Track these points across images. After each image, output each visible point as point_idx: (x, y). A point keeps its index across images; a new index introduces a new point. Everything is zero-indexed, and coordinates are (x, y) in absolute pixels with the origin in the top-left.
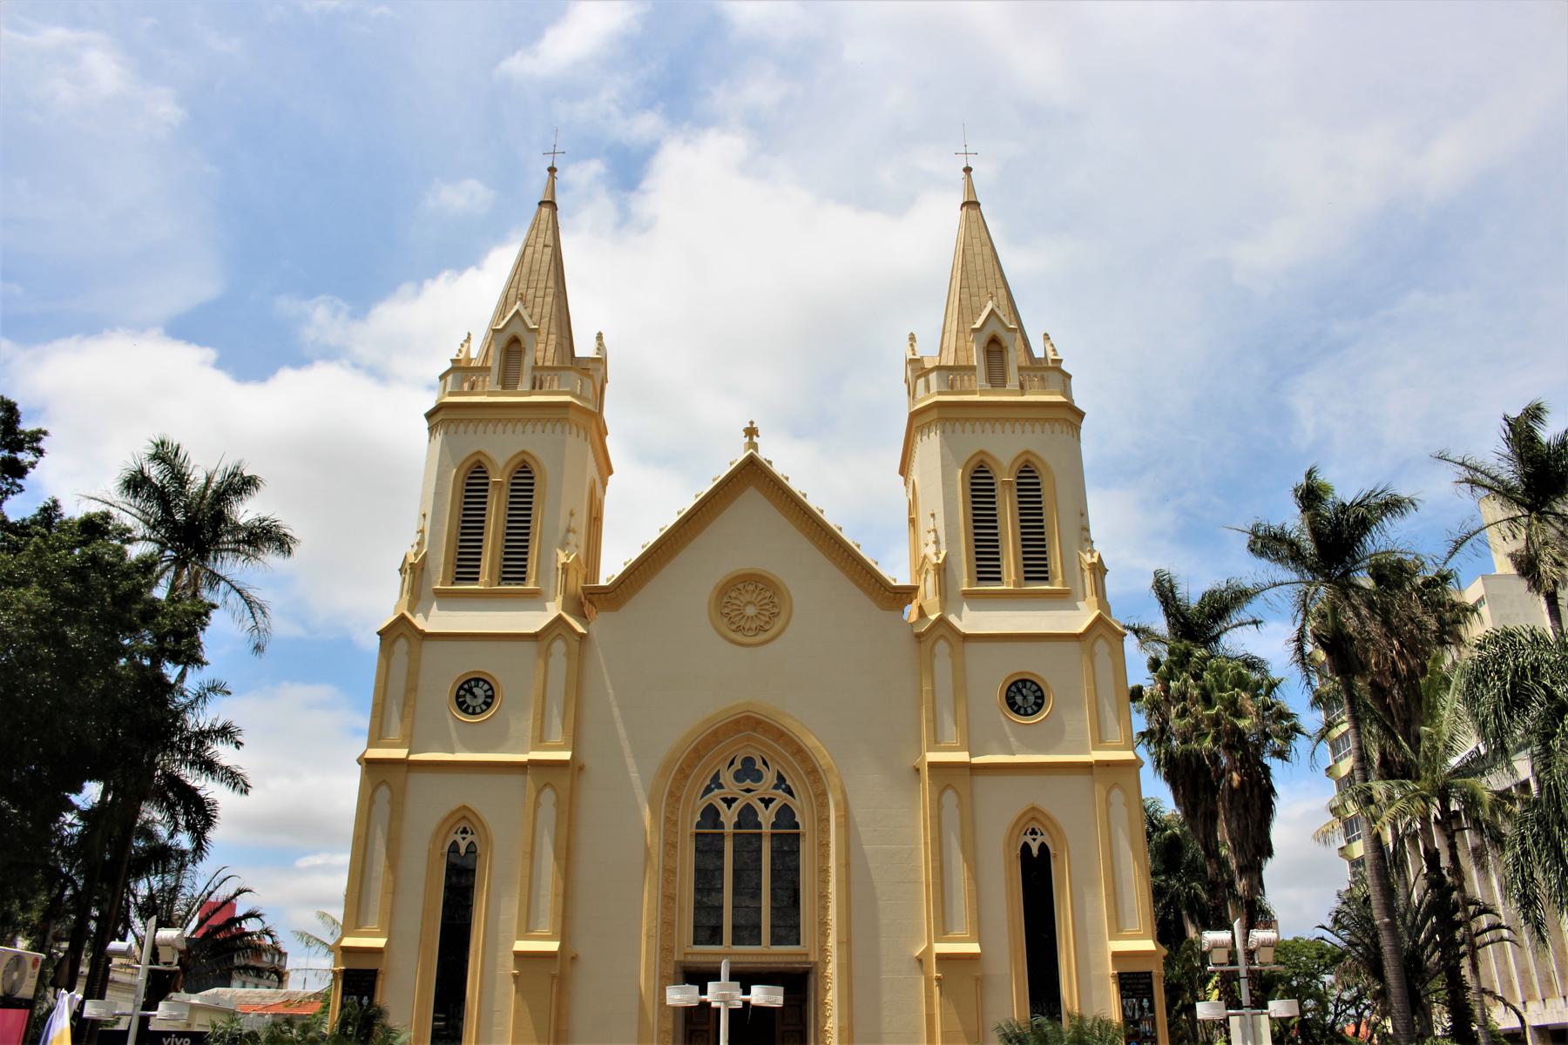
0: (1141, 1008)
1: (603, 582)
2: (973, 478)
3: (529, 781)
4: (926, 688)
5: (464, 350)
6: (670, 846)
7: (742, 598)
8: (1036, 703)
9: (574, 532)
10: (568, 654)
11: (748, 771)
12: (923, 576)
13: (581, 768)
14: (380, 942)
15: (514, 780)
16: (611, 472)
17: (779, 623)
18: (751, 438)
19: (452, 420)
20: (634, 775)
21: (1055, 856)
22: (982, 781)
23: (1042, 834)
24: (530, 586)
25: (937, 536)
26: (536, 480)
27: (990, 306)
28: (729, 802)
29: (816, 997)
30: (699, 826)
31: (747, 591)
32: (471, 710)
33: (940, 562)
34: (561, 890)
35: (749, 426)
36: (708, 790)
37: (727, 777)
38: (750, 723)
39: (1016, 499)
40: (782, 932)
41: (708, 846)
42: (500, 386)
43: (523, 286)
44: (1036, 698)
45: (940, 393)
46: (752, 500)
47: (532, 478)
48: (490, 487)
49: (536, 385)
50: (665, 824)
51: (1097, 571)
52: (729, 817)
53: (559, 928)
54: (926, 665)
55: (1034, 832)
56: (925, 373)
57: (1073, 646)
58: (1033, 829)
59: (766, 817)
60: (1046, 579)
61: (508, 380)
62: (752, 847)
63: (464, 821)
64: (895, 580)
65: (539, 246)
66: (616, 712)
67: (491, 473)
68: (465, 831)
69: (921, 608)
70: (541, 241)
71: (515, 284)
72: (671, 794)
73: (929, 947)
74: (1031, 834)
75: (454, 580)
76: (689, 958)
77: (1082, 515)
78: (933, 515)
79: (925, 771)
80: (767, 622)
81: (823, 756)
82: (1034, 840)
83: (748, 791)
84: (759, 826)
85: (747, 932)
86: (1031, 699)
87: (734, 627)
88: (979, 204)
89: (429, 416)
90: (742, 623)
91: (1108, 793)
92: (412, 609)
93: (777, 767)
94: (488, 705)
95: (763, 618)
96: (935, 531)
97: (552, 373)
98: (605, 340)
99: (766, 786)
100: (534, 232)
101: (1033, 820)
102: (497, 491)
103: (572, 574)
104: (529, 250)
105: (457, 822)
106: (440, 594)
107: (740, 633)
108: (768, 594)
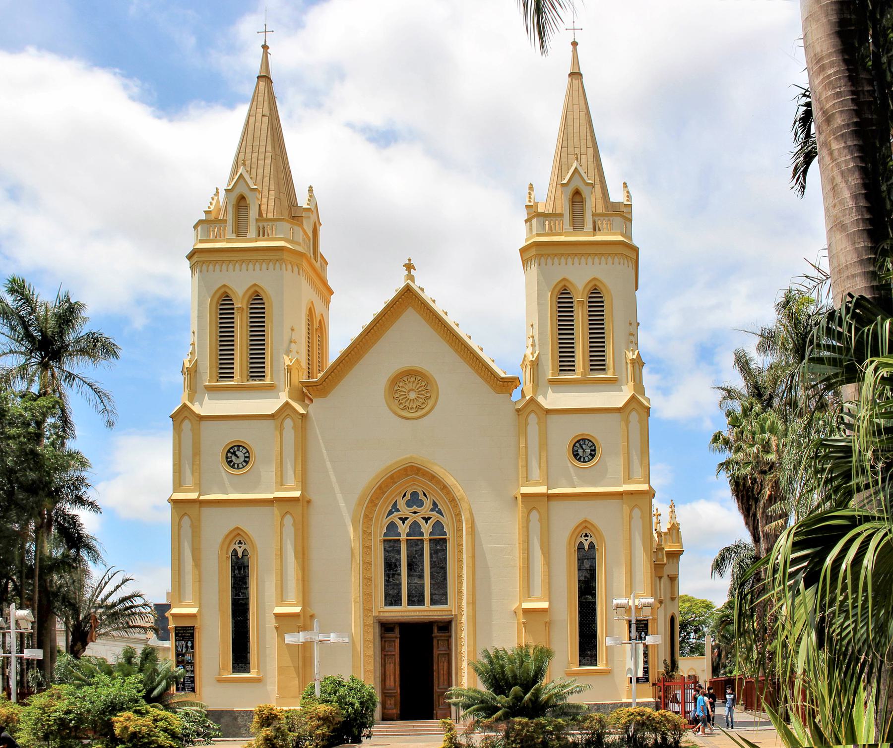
3: (276, 511)
4: (522, 445)
6: (367, 549)
8: (591, 454)
9: (295, 342)
10: (294, 428)
11: (414, 500)
12: (524, 369)
13: (309, 502)
14: (194, 611)
15: (266, 510)
17: (431, 402)
18: (409, 272)
19: (204, 262)
20: (342, 505)
21: (598, 550)
22: (554, 504)
23: (591, 537)
24: (267, 381)
25: (534, 341)
27: (575, 165)
28: (404, 520)
29: (456, 634)
30: (385, 535)
31: (409, 382)
32: (236, 466)
33: (534, 359)
34: (301, 578)
36: (390, 513)
37: (402, 504)
38: (413, 470)
39: (586, 313)
40: (436, 597)
41: (391, 547)
43: (249, 151)
44: (591, 450)
45: (538, 235)
46: (410, 317)
49: (262, 233)
50: (362, 535)
51: (637, 366)
52: (403, 529)
53: (301, 599)
54: (522, 430)
57: (617, 416)
58: (586, 534)
59: (426, 529)
60: (604, 370)
61: (240, 231)
62: (418, 548)
63: (238, 536)
64: (505, 373)
65: (259, 116)
66: (329, 465)
67: (234, 301)
69: (522, 390)
71: (243, 149)
72: (366, 516)
73: (520, 605)
74: (585, 536)
75: (218, 378)
78: (532, 325)
79: (519, 498)
80: (423, 403)
81: (459, 490)
82: (586, 540)
83: (415, 513)
84: (422, 534)
85: (416, 598)
86: (588, 451)
87: (402, 407)
89: (190, 257)
90: (407, 404)
91: (631, 511)
92: (191, 400)
93: (432, 498)
94: (247, 462)
96: (533, 337)
97: (270, 224)
99: (425, 510)
100: (255, 103)
101: (585, 529)
102: (240, 314)
103: (294, 372)
104: (252, 120)
105: (235, 537)
106: (209, 389)
107: (405, 411)
108: (423, 384)
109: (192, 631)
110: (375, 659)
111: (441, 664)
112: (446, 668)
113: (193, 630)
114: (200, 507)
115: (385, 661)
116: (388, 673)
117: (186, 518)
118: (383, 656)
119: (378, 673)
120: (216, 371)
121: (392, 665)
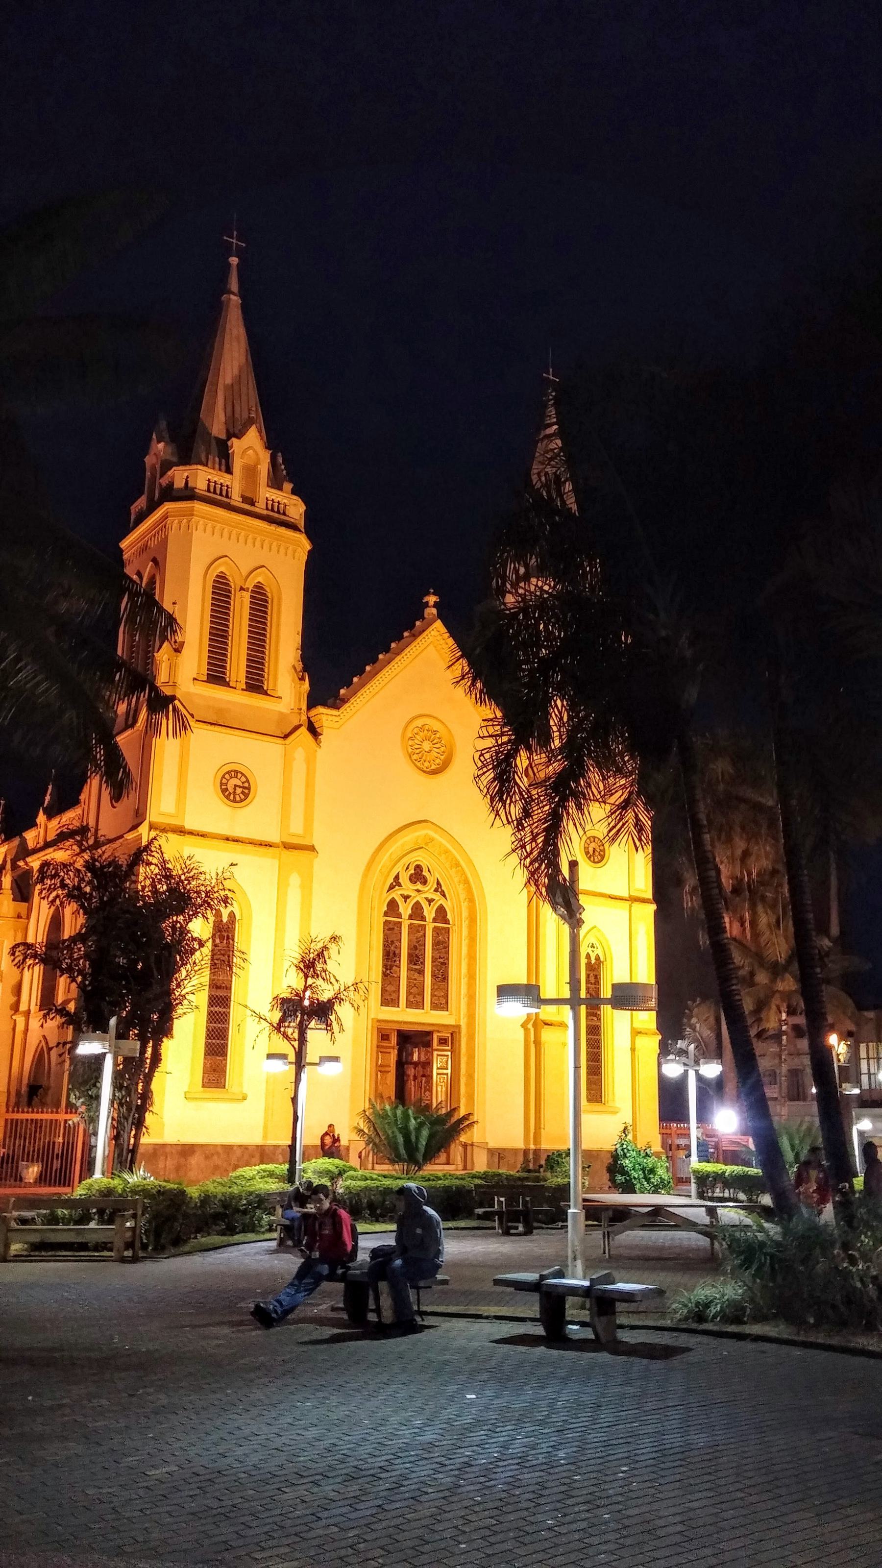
30: (386, 914)
36: (391, 887)
41: (391, 932)
52: (405, 910)
59: (429, 913)
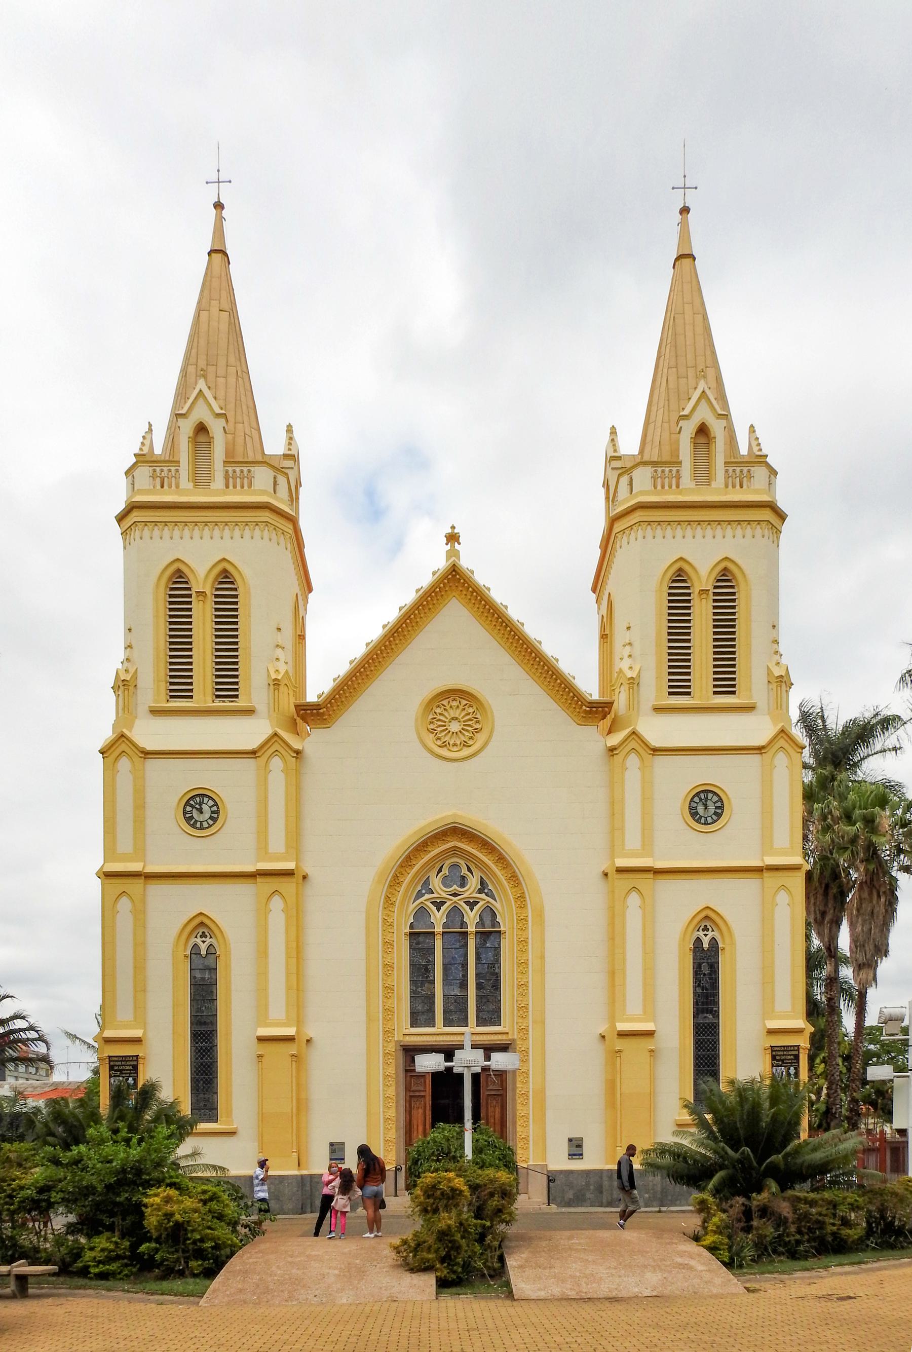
0: (789, 1074)
1: (312, 697)
2: (670, 588)
5: (147, 442)
7: (445, 713)
8: (715, 813)
10: (286, 771)
16: (310, 590)
17: (481, 738)
21: (723, 949)
23: (713, 931)
24: (241, 703)
26: (240, 592)
28: (439, 905)
35: (450, 531)
42: (192, 484)
44: (717, 808)
47: (235, 589)
48: (193, 599)
52: (438, 919)
55: (706, 929)
56: (626, 471)
59: (471, 918)
68: (203, 935)
70: (214, 303)
75: (168, 697)
76: (407, 1038)
77: (774, 626)
80: (471, 738)
83: (455, 895)
86: (712, 809)
88: (694, 259)
90: (447, 739)
93: (480, 874)
94: (215, 820)
95: (467, 734)
98: (296, 434)
107: (445, 749)
108: (471, 710)
109: (135, 1063)
110: (397, 1102)
111: (491, 1110)
112: (498, 1115)
113: (137, 1060)
114: (145, 884)
115: (410, 1105)
116: (414, 1122)
117: (124, 900)
118: (408, 1098)
119: (402, 1123)
120: (164, 687)
121: (421, 1111)
